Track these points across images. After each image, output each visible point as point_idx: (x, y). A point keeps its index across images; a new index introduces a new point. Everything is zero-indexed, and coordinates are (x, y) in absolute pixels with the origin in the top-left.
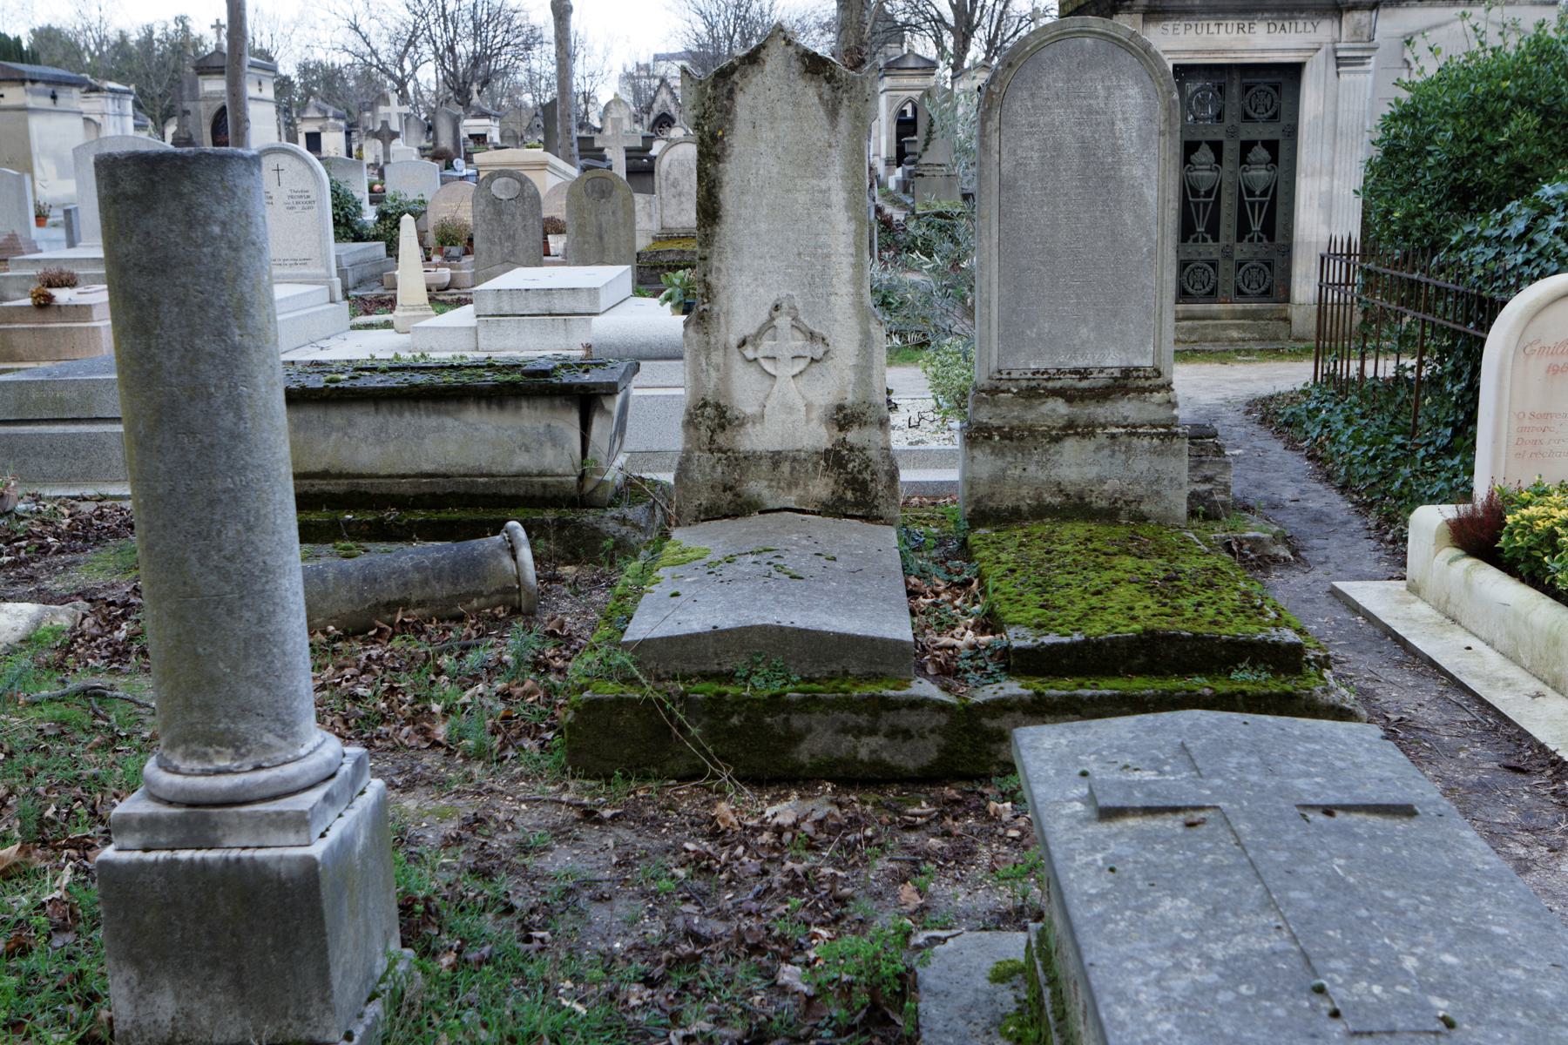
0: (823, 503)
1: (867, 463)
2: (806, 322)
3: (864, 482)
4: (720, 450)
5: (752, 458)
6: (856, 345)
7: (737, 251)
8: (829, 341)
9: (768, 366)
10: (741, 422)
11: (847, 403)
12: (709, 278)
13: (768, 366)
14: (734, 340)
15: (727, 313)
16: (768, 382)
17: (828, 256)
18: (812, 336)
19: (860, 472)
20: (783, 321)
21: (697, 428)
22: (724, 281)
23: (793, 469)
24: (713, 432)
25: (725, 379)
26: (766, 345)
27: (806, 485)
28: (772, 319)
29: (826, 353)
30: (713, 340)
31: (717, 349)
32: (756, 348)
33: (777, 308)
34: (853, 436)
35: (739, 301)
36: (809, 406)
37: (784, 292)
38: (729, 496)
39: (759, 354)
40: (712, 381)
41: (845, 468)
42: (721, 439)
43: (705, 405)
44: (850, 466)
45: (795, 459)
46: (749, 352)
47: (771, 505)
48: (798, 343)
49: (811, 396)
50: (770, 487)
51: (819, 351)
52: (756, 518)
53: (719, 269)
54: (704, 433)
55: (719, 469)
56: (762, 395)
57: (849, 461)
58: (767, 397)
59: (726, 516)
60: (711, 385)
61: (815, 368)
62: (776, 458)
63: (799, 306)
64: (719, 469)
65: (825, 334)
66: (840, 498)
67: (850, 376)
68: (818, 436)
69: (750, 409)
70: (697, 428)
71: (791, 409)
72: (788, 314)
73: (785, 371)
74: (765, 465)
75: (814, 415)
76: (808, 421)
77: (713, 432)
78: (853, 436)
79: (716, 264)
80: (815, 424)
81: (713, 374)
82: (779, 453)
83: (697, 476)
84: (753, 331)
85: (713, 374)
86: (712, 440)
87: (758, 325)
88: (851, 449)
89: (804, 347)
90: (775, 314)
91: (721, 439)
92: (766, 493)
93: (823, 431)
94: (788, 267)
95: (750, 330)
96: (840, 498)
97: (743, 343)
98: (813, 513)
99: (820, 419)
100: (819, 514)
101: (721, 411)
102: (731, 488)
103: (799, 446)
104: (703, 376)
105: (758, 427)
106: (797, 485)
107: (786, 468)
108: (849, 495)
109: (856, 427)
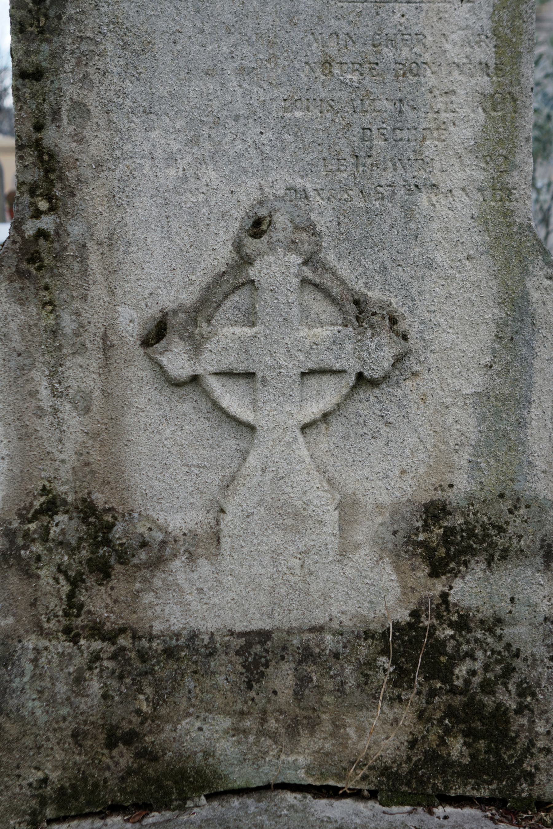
0: (385, 771)
1: (507, 661)
2: (344, 269)
3: (501, 711)
4: (97, 631)
5: (188, 652)
6: (485, 334)
7: (137, 50)
8: (410, 324)
9: (232, 399)
10: (156, 553)
11: (454, 497)
12: (50, 137)
13: (232, 399)
14: (130, 323)
15: (110, 242)
16: (232, 443)
17: (412, 69)
18: (360, 312)
19: (487, 687)
20: (277, 268)
21: (29, 574)
22: (96, 147)
23: (303, 681)
24: (76, 582)
25: (108, 434)
26: (227, 337)
27: (338, 725)
28: (244, 260)
29: (399, 359)
30: (68, 324)
31: (80, 349)
32: (196, 347)
33: (257, 227)
34: (469, 589)
35: (143, 207)
36: (348, 509)
37: (281, 180)
38: (124, 757)
39: (205, 365)
40: (68, 442)
41: (446, 675)
42: (98, 602)
43: (52, 506)
44: (461, 670)
45: (307, 655)
46: (177, 360)
47: (239, 777)
48: (319, 333)
49: (353, 480)
50: (236, 731)
51: (381, 354)
52: (203, 810)
53: (81, 110)
54: (50, 585)
55: (95, 687)
56: (215, 479)
57: (458, 657)
58: (229, 484)
59: (115, 809)
60: (68, 453)
61: (367, 404)
62: (256, 651)
63: (323, 223)
64: (95, 687)
65: (397, 303)
66: (432, 757)
67: (465, 423)
68: (370, 589)
69: (180, 517)
70: (29, 574)
71: (295, 518)
72: (292, 245)
73: (281, 411)
74: (225, 672)
75: (362, 532)
76: (343, 553)
77: (76, 582)
78: (469, 589)
79: (71, 91)
80: (363, 557)
81: (73, 420)
82: (264, 636)
83: (33, 706)
84: (188, 297)
85: (73, 420)
86: (73, 606)
87: (201, 278)
88: (463, 624)
89: (338, 343)
90: (252, 245)
91: (98, 602)
92: (227, 748)
93: (387, 577)
94: (292, 102)
95: (179, 294)
96: (432, 757)
97: (157, 333)
98: (356, 794)
99: (378, 543)
100: (373, 795)
101: (97, 522)
102: (130, 738)
103: (319, 617)
104: (43, 427)
105: (204, 567)
106: (313, 725)
107: (282, 679)
108: (457, 748)
109: (478, 567)
